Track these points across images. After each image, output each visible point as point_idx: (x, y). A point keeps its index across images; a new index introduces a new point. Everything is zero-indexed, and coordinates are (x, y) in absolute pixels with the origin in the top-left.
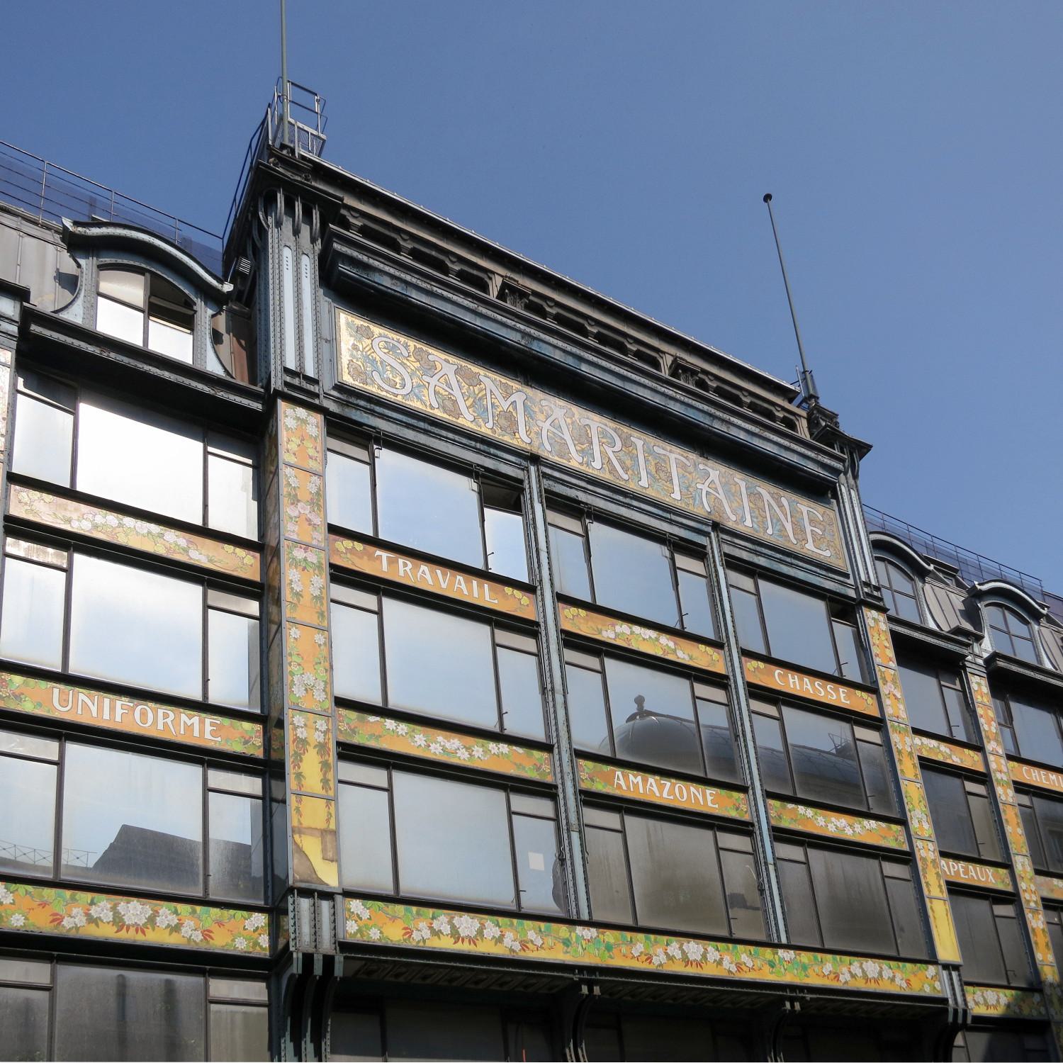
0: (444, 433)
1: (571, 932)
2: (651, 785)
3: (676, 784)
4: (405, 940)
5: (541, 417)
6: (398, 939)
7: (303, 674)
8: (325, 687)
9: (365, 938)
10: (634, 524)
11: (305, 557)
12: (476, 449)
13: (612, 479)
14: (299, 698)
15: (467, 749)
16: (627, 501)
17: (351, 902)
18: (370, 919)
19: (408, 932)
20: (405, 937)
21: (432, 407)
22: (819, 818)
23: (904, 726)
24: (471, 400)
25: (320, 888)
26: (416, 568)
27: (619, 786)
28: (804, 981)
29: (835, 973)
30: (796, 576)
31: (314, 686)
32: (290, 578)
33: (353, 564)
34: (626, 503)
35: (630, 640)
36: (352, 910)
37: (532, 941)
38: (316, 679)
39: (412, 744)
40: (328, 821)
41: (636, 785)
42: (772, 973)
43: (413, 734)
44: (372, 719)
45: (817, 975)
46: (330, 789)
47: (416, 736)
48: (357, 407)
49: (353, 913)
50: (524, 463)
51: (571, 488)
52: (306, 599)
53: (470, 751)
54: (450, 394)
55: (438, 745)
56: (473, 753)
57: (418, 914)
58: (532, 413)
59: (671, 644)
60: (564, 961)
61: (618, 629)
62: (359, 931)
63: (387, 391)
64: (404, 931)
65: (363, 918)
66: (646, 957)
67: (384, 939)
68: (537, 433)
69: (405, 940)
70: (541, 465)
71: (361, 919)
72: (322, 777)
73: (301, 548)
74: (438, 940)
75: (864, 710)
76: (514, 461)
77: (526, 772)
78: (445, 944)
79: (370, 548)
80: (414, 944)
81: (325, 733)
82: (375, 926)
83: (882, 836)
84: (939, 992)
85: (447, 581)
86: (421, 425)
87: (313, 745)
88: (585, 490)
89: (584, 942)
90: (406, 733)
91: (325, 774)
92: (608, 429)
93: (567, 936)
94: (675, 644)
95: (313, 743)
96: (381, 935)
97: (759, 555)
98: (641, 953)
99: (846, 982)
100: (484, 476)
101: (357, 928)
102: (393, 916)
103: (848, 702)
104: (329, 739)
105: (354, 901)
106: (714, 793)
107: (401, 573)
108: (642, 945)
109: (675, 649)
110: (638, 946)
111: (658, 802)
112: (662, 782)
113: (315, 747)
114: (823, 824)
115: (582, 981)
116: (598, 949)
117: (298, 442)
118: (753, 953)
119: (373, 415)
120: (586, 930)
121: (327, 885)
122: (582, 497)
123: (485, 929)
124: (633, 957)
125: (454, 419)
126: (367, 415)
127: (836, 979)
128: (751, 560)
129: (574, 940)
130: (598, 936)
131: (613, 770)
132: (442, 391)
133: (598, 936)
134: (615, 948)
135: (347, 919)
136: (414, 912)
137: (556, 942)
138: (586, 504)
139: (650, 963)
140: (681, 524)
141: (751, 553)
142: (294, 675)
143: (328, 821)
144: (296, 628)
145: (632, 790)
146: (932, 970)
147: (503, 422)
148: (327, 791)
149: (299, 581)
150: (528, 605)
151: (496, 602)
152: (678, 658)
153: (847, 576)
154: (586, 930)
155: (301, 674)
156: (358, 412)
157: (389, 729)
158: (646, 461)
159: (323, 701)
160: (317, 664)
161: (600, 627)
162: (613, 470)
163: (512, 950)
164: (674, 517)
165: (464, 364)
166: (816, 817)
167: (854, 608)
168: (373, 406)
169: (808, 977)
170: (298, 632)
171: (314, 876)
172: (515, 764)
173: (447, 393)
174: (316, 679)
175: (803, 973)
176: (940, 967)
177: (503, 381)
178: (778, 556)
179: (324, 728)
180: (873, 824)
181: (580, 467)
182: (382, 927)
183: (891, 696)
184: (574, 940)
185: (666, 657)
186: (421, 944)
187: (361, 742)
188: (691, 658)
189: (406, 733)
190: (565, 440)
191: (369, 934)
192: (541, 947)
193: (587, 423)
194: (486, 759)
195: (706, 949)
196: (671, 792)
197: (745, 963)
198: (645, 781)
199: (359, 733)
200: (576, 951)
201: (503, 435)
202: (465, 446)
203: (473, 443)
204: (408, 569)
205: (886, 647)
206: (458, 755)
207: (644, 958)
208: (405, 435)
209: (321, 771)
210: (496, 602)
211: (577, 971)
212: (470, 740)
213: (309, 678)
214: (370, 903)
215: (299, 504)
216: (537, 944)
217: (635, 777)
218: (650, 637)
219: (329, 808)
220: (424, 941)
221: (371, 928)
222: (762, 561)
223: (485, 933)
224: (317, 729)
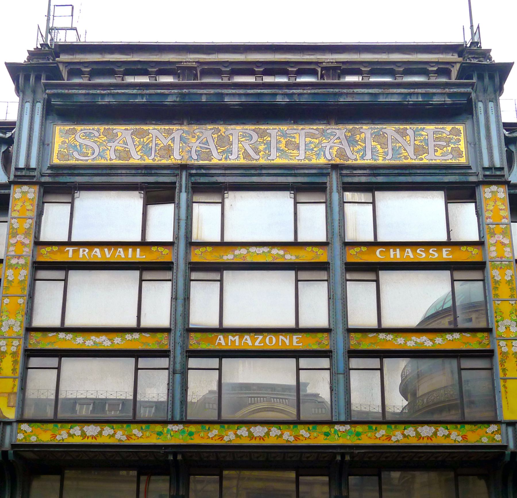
0: (119, 172)
1: (163, 428)
2: (246, 340)
3: (267, 336)
4: (51, 440)
5: (194, 140)
6: (47, 440)
7: (9, 320)
8: (21, 324)
9: (27, 441)
10: (266, 185)
11: (18, 262)
12: (143, 174)
13: (246, 162)
14: (5, 332)
15: (110, 340)
16: (258, 172)
17: (22, 425)
18: (32, 432)
19: (54, 436)
20: (51, 439)
21: (111, 159)
22: (398, 339)
23: (507, 263)
24: (140, 147)
25: (4, 420)
26: (91, 251)
27: (220, 344)
28: (355, 443)
29: (387, 436)
30: (414, 181)
31: (14, 325)
32: (8, 275)
33: (50, 258)
34: (257, 174)
35: (246, 257)
36: (22, 429)
37: (135, 435)
38: (16, 321)
39: (74, 343)
40: (13, 388)
41: (233, 342)
42: (326, 439)
43: (76, 338)
44: (51, 335)
45: (369, 438)
46: (17, 373)
47: (77, 339)
48: (62, 175)
49: (22, 430)
50: (176, 172)
51: (213, 176)
52: (15, 284)
53: (112, 341)
54: (126, 148)
55: (92, 341)
56: (114, 342)
57: (61, 427)
58: (186, 140)
59: (281, 252)
60: (155, 443)
61: (237, 252)
62: (25, 438)
63: (81, 160)
64: (52, 436)
65: (28, 432)
66: (219, 437)
67: (39, 440)
68: (188, 152)
69: (51, 440)
70: (189, 169)
71: (26, 432)
72: (12, 367)
73: (16, 258)
74: (72, 439)
75: (467, 259)
76: (170, 173)
77: (150, 346)
78: (77, 440)
79: (62, 248)
80: (57, 441)
81: (17, 346)
82: (34, 435)
83: (464, 343)
84: (498, 441)
85: (111, 254)
86: (104, 172)
87: (9, 354)
88: (224, 175)
89: (172, 433)
90: (71, 338)
91: (14, 367)
92: (247, 131)
93: (161, 430)
94: (285, 251)
95: (9, 352)
96: (37, 439)
97: (377, 176)
98: (215, 435)
99: (398, 441)
100: (147, 188)
101: (23, 437)
102: (45, 430)
103: (451, 257)
104: (19, 349)
105: (24, 424)
106: (301, 337)
107: (81, 256)
108: (217, 431)
109: (284, 255)
110: (213, 432)
111: (254, 348)
112: (255, 337)
113: (10, 355)
114: (402, 342)
115: (166, 454)
116: (183, 436)
117: (22, 204)
118: (311, 429)
119: (72, 176)
120: (175, 426)
121: (8, 418)
122: (221, 179)
123: (104, 431)
124: (209, 438)
125: (126, 162)
126: (70, 177)
127: (388, 439)
128: (369, 181)
129: (165, 432)
130: (184, 429)
131: (216, 335)
132: (120, 148)
133: (184, 429)
134: (196, 434)
135: (18, 433)
136: (59, 427)
137: (152, 434)
138: (224, 183)
139: (221, 440)
140: (305, 174)
141: (370, 176)
142: (3, 321)
143: (13, 388)
144: (7, 298)
145: (229, 344)
146: (494, 428)
147: (163, 152)
148: (14, 375)
149: (12, 275)
150: (167, 254)
151: (144, 257)
152: (286, 259)
153: (469, 168)
154: (175, 426)
155: (7, 320)
156: (64, 177)
157: (61, 338)
158: (278, 142)
159: (18, 331)
160: (17, 314)
161: (222, 254)
162: (246, 155)
163: (120, 440)
164: (296, 172)
165: (138, 127)
166: (396, 339)
167: (475, 188)
168: (72, 171)
169: (360, 440)
170: (8, 300)
171: (1, 415)
172: (143, 343)
173: (123, 148)
174: (16, 321)
175: (356, 438)
176: (504, 426)
177: (167, 127)
178: (396, 171)
179: (18, 344)
180: (457, 336)
181: (220, 162)
182: (38, 435)
183: (498, 243)
184: (165, 432)
185: (275, 261)
186: (61, 441)
187: (42, 347)
188: (297, 257)
189: (71, 338)
190: (210, 149)
191: (30, 439)
192: (141, 437)
193: (231, 133)
194: (122, 343)
195: (270, 430)
196: (271, 340)
197: (302, 435)
198: (241, 338)
199: (41, 343)
200: (166, 438)
201: (161, 160)
202: (134, 175)
203: (140, 171)
204: (85, 253)
205: (501, 210)
206: (103, 344)
207: (217, 437)
208: (94, 180)
209: (13, 365)
210: (144, 257)
211: (163, 448)
212: (112, 335)
213: (12, 321)
214: (32, 425)
215: (17, 236)
216: (138, 436)
217: (234, 337)
218: (263, 252)
219: (15, 382)
220: (63, 440)
221: (32, 436)
222: (380, 179)
223: (103, 433)
224: (13, 345)
